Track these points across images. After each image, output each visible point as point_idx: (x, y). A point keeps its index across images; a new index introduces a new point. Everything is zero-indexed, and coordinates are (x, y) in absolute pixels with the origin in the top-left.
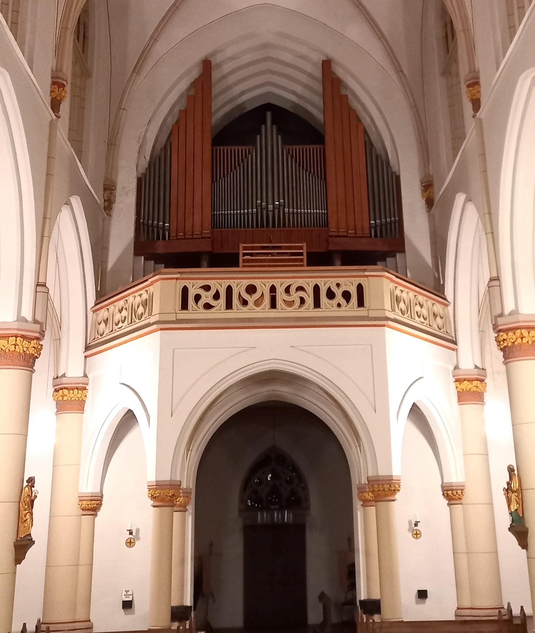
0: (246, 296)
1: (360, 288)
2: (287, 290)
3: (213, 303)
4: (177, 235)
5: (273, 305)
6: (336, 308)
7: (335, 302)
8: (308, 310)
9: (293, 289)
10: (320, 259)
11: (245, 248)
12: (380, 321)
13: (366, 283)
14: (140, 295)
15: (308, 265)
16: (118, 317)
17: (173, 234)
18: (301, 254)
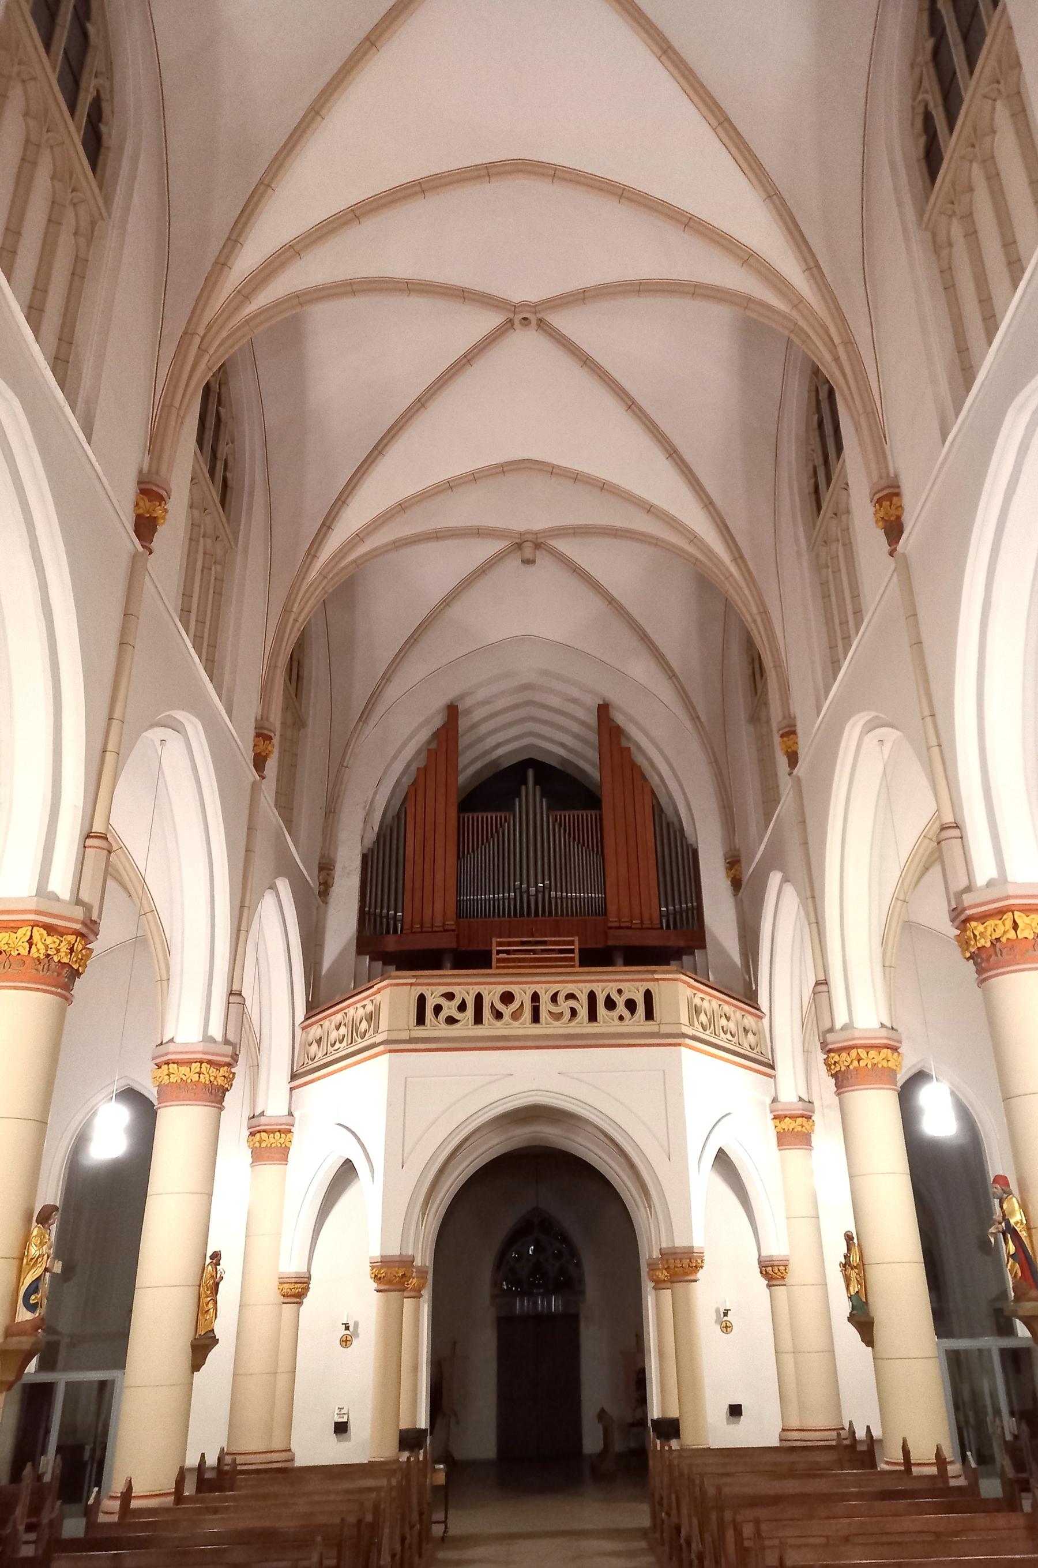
0: (500, 1007)
1: (648, 996)
2: (554, 998)
3: (457, 1015)
4: (412, 927)
5: (536, 1018)
6: (617, 1022)
7: (615, 1014)
8: (582, 1025)
9: (561, 998)
10: (596, 957)
11: (499, 944)
12: (674, 1038)
13: (657, 990)
14: (364, 1007)
15: (580, 966)
16: (334, 1035)
17: (407, 926)
18: (572, 951)
